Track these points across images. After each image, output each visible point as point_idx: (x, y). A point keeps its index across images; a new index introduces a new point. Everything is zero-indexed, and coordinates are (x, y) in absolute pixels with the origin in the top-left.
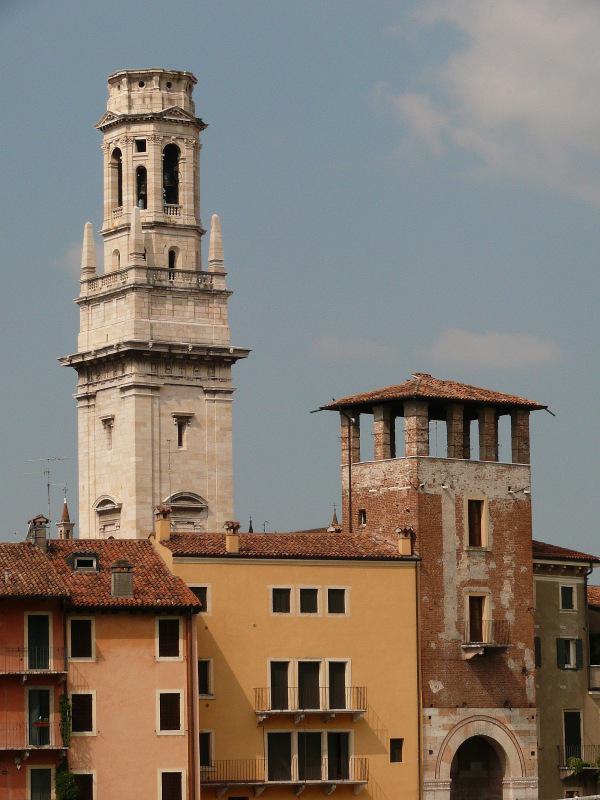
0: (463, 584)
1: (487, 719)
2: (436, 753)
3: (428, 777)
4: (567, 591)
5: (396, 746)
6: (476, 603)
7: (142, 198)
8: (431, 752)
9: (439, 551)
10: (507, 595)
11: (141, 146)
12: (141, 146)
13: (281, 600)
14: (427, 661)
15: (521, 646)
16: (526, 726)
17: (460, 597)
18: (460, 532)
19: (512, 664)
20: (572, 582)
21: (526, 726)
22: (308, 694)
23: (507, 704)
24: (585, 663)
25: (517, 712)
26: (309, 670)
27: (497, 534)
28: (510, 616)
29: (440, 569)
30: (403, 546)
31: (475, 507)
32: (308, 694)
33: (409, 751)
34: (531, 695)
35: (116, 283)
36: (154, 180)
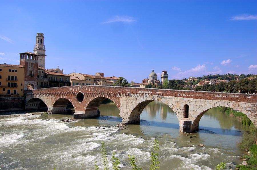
3: (24, 87)
4: (42, 72)
6: (31, 72)
7: (39, 42)
9: (27, 67)
10: (35, 71)
11: (39, 39)
12: (39, 39)
13: (10, 71)
14: (25, 77)
17: (29, 72)
18: (30, 65)
19: (35, 78)
20: (43, 71)
23: (34, 81)
25: (35, 82)
26: (13, 77)
27: (34, 66)
28: (35, 73)
33: (23, 85)
35: (36, 49)
36: (40, 41)
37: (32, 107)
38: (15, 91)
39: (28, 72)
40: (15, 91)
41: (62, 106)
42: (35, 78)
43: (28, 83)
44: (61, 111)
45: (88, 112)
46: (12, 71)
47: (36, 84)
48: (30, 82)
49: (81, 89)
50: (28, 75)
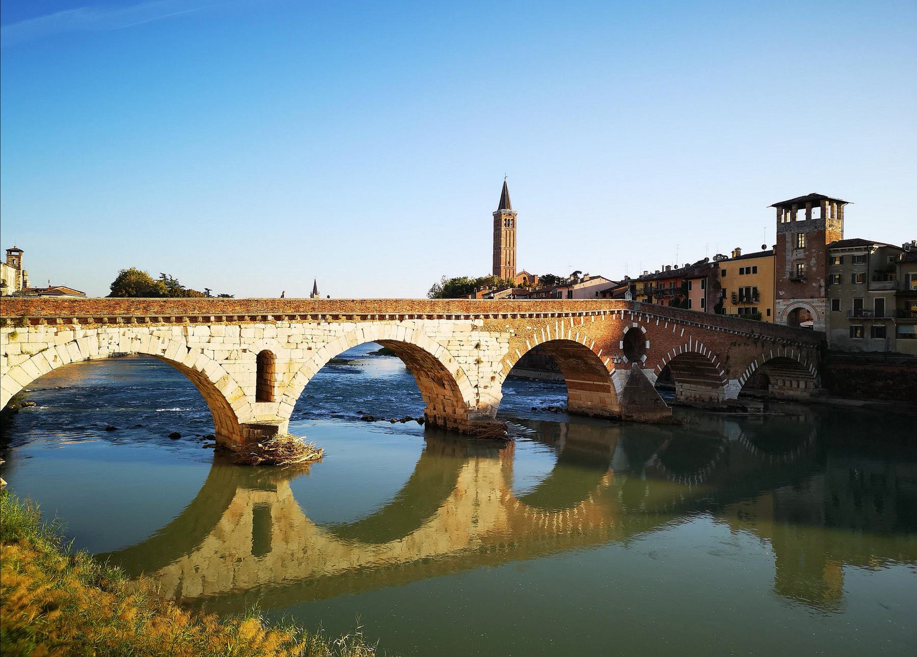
0: (794, 261)
1: (803, 302)
2: (781, 313)
8: (779, 313)
10: (813, 261)
13: (741, 271)
14: (778, 286)
15: (819, 278)
16: (820, 304)
19: (814, 284)
21: (820, 304)
23: (812, 297)
24: (867, 282)
26: (748, 289)
28: (814, 269)
29: (785, 257)
30: (774, 253)
34: (823, 294)
37: (791, 393)
39: (788, 268)
42: (814, 284)
43: (788, 306)
44: (703, 401)
46: (747, 273)
47: (819, 310)
48: (793, 303)
50: (788, 276)
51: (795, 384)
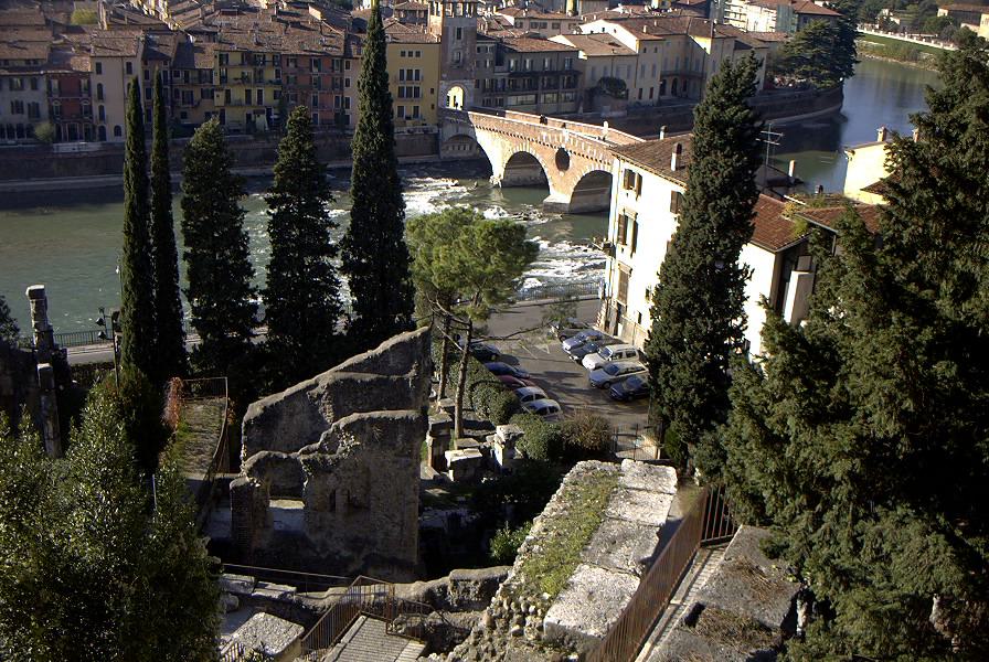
5: (432, 91)
10: (468, 51)
13: (403, 54)
14: (442, 69)
22: (410, 78)
26: (410, 72)
28: (468, 57)
31: (459, 30)
32: (410, 78)
33: (435, 92)
37: (460, 155)
38: (416, 108)
40: (416, 108)
41: (530, 168)
45: (581, 198)
49: (567, 139)
51: (462, 148)
